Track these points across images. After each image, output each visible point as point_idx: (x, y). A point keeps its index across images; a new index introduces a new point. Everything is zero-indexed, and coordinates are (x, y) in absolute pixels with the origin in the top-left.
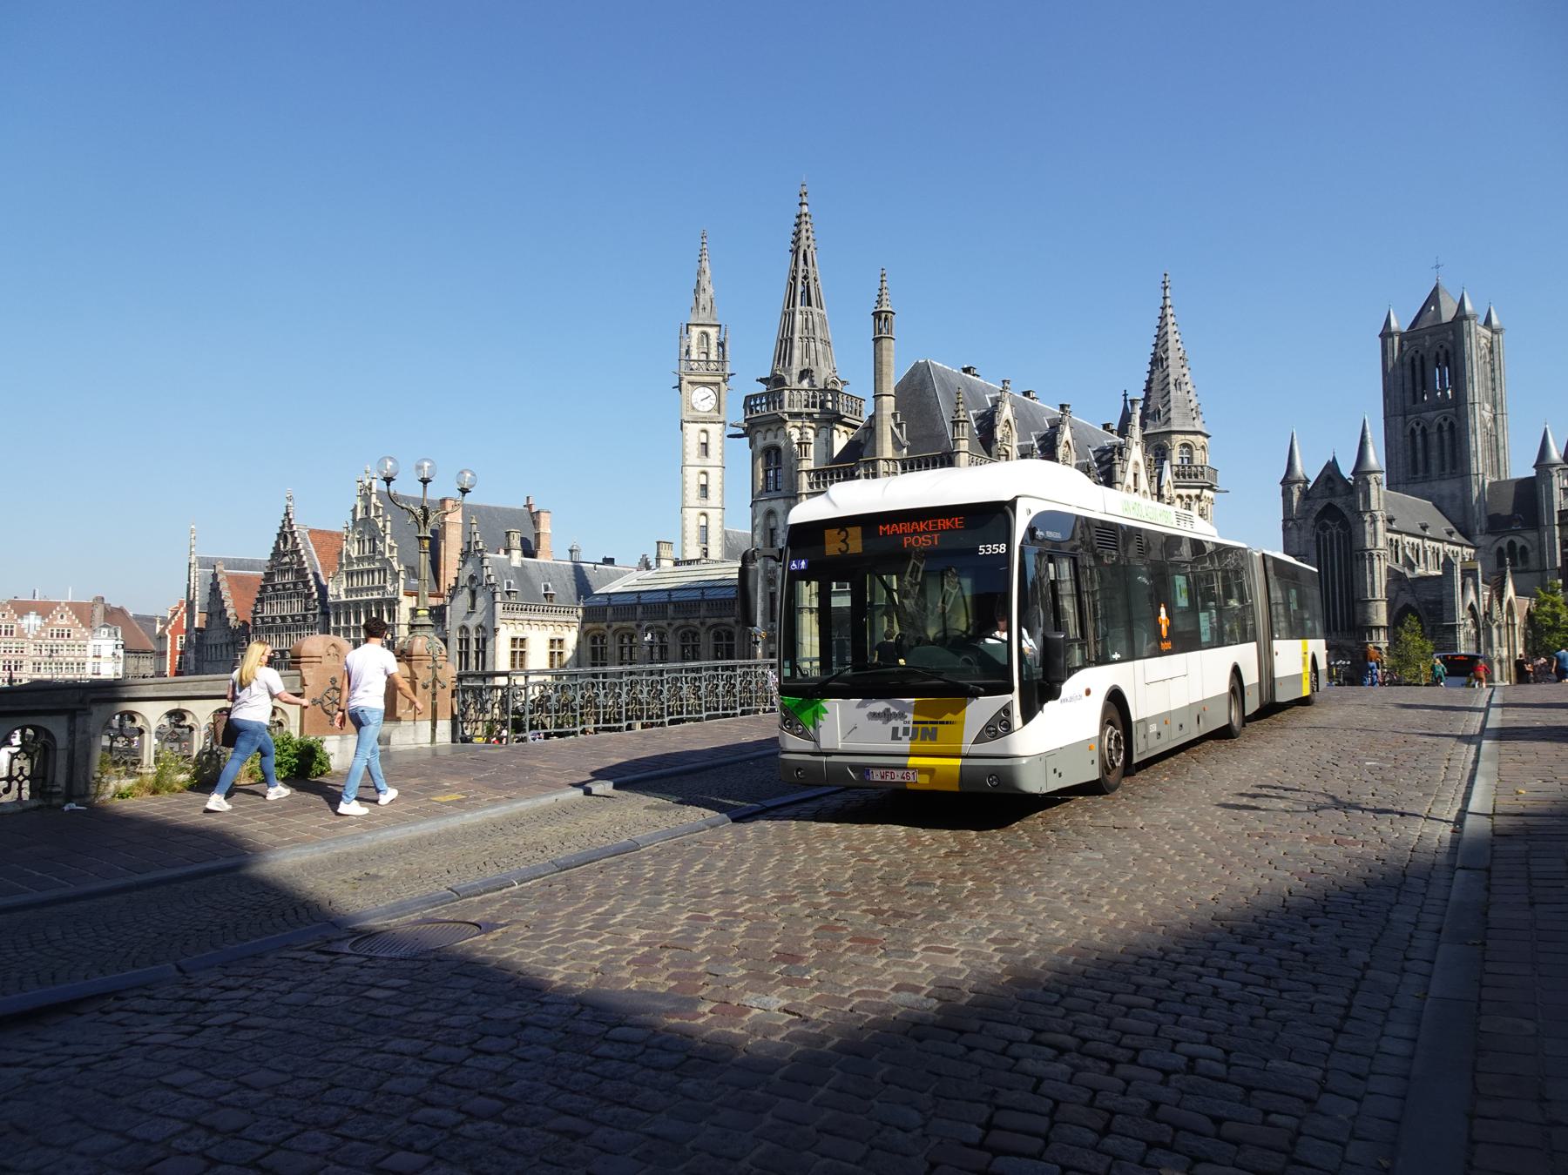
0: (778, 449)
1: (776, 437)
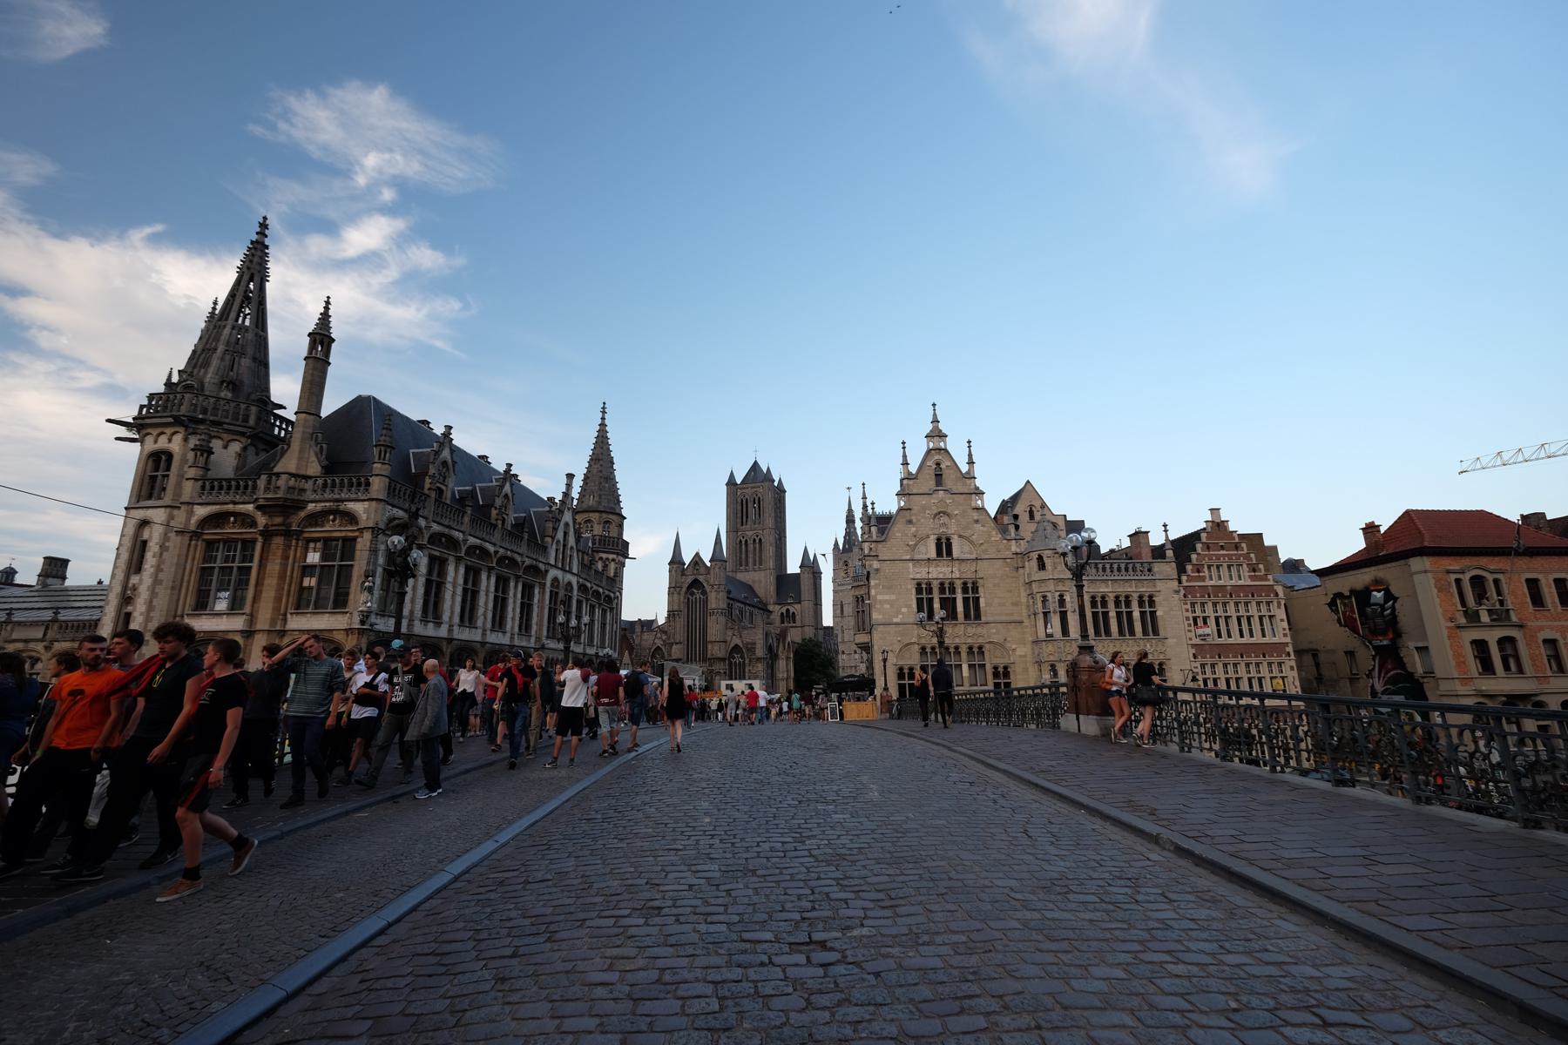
0: (170, 456)
1: (170, 440)
